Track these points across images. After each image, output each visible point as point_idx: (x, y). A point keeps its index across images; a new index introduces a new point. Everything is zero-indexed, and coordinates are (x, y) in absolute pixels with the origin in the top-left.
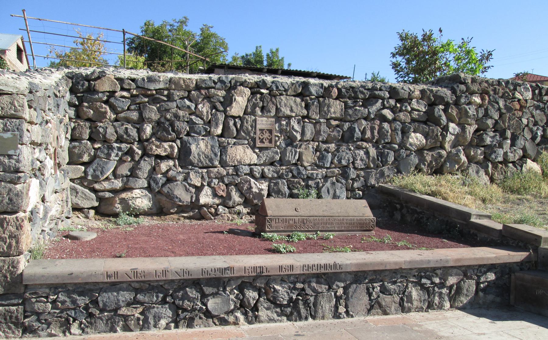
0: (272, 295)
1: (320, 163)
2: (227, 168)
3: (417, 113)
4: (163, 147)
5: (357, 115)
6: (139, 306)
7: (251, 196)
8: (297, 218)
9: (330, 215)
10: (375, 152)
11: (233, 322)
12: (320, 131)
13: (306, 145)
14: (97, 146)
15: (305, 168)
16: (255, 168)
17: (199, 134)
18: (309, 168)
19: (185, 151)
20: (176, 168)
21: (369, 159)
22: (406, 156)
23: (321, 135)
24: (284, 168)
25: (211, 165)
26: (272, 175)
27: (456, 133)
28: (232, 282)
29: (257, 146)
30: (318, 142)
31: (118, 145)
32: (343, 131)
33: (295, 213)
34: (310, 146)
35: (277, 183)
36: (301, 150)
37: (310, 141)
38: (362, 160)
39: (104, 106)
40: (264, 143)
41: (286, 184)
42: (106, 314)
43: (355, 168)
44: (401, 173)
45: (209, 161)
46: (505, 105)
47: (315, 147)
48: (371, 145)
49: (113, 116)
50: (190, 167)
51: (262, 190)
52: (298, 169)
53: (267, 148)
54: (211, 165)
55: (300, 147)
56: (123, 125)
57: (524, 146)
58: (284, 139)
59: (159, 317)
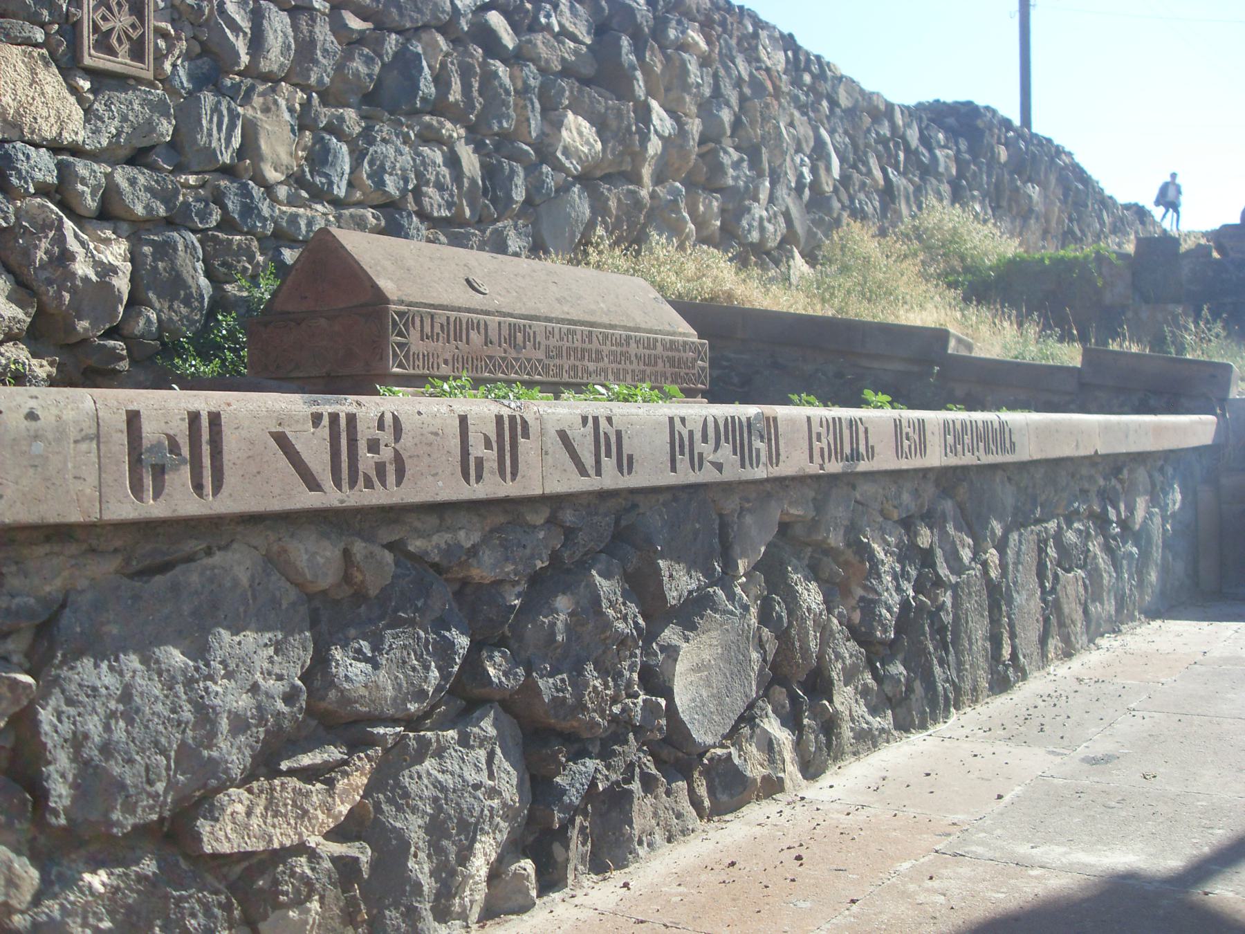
0: (860, 592)
1: (317, 179)
3: (572, 45)
5: (419, 11)
6: (334, 753)
7: (67, 296)
8: (493, 320)
9: (588, 318)
10: (475, 159)
11: (764, 778)
12: (313, 42)
13: (263, 94)
15: (269, 189)
16: (82, 167)
18: (282, 192)
21: (460, 187)
22: (557, 191)
23: (316, 62)
24: (192, 180)
27: (667, 134)
28: (749, 519)
29: (87, 61)
30: (305, 88)
32: (384, 64)
33: (475, 300)
34: (282, 103)
36: (250, 112)
37: (277, 81)
38: (440, 187)
40: (112, 52)
42: (98, 880)
43: (424, 216)
44: (547, 252)
46: (751, 75)
47: (297, 107)
48: (462, 132)
51: (113, 270)
52: (245, 193)
53: (121, 81)
55: (247, 100)
57: (787, 208)
58: (187, 56)
59: (463, 826)
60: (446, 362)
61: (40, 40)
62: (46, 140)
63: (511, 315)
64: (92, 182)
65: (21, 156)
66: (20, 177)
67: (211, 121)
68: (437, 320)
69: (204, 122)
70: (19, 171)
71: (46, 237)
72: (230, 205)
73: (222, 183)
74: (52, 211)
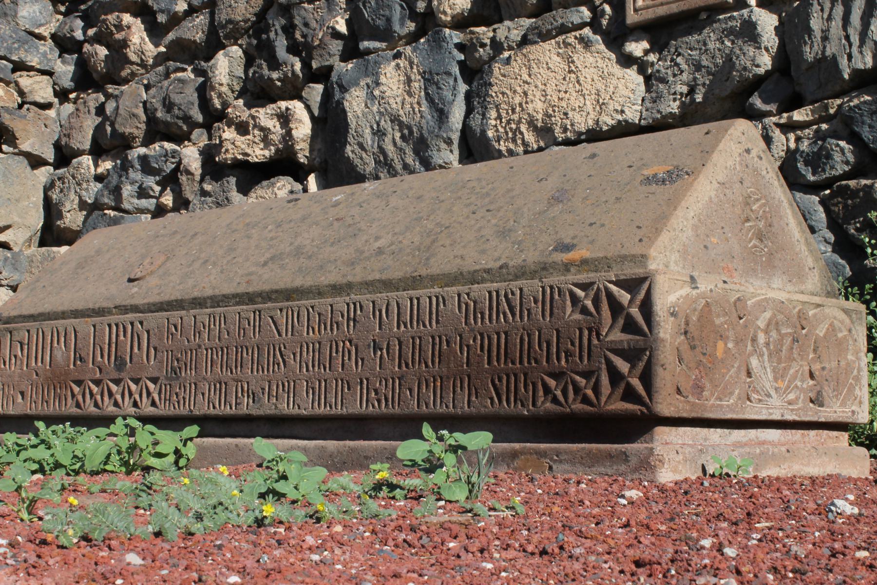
4: (255, 126)
14: (107, 165)
17: (385, 34)
19: (331, 122)
31: (142, 150)
39: (127, 18)
45: (416, 152)
49: (151, 50)
56: (167, 75)
60: (22, 394)
61: (577, 20)
62: (582, 133)
67: (830, 18)
68: (16, 337)
69: (816, 24)
72: (866, 134)
73: (856, 102)
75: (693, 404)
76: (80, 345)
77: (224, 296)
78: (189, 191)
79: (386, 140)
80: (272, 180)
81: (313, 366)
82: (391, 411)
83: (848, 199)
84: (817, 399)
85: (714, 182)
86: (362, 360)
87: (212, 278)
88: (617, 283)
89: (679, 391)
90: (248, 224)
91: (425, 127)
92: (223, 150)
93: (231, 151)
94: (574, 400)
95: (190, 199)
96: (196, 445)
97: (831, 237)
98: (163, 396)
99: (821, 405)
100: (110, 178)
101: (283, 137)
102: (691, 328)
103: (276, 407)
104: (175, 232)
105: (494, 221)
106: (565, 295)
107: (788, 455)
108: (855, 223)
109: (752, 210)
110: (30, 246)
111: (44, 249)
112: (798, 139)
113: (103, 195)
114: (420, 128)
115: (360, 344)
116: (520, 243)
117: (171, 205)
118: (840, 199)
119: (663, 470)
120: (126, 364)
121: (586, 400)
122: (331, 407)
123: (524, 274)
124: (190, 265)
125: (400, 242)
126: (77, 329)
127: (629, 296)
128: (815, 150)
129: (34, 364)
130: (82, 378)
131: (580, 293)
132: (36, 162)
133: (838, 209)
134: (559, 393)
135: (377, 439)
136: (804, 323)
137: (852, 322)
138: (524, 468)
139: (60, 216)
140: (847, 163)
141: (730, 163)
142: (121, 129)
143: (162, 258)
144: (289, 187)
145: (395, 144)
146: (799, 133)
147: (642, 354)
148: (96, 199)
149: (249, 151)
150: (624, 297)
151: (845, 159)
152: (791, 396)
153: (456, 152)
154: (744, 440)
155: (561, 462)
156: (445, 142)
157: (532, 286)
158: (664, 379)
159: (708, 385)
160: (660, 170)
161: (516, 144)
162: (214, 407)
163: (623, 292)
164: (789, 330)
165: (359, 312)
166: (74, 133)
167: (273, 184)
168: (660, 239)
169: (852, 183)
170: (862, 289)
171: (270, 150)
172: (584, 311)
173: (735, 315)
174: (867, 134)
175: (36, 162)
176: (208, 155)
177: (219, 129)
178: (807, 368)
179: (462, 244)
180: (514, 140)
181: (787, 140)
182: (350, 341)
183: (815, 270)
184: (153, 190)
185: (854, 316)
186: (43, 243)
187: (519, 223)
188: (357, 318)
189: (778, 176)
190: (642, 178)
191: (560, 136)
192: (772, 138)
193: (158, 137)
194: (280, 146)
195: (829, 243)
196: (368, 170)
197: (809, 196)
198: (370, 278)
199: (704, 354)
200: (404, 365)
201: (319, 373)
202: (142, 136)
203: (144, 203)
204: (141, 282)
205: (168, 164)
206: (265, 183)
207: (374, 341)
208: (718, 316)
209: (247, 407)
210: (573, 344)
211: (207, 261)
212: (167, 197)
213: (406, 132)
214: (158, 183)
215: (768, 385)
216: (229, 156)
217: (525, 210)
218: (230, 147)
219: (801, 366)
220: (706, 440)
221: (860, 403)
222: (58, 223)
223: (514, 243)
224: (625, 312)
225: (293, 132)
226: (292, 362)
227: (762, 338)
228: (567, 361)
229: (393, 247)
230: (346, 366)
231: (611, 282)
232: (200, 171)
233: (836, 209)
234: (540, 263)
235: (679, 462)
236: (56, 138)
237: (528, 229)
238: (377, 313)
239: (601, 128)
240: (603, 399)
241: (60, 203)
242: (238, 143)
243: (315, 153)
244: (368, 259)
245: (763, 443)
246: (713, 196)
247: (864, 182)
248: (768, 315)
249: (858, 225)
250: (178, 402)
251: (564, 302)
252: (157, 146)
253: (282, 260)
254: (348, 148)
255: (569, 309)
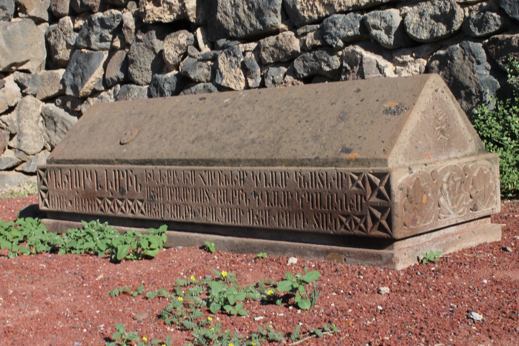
2: (301, 31)
4: (164, 2)
14: (80, 23)
20: (200, 50)
25: (259, 26)
26: (432, 31)
31: (100, 15)
35: (447, 54)
41: (483, 54)
45: (257, 17)
50: (222, 42)
54: (259, 26)
60: (71, 202)
63: (126, 162)
64: (384, 25)
65: (330, 24)
66: (332, 37)
68: (64, 172)
70: (331, 35)
71: (353, 72)
72: (508, 9)
74: (357, 53)
75: (413, 229)
76: (99, 179)
77: (174, 160)
78: (130, 39)
79: (239, 10)
80: (177, 33)
81: (224, 201)
82: (265, 226)
83: (497, 46)
84: (474, 208)
85: (420, 113)
86: (249, 200)
87: (166, 147)
88: (373, 174)
89: (405, 225)
90: (180, 113)
91: (261, 3)
92: (147, 16)
93: (152, 16)
94: (355, 228)
95: (131, 43)
96: (166, 235)
97: (489, 66)
98: (147, 209)
99: (476, 210)
100: (82, 31)
101: (181, 8)
102: (410, 193)
103: (207, 220)
104: (140, 113)
105: (310, 129)
106: (348, 178)
107: (460, 240)
108: (502, 59)
109: (439, 121)
110: (41, 70)
111: (49, 72)
112: (470, 11)
113: (80, 41)
114: (259, 4)
115: (247, 192)
116: (324, 145)
117: (119, 46)
118: (493, 46)
119: (399, 264)
120: (125, 191)
121: (360, 229)
122: (235, 222)
123: (327, 163)
124: (153, 138)
125: (263, 137)
126: (97, 171)
127: (379, 181)
128: (480, 18)
129: (75, 187)
130: (102, 197)
131: (356, 177)
132: (38, 21)
133: (492, 51)
134: (347, 224)
135: (259, 238)
136: (466, 172)
137: (492, 163)
138: (333, 259)
139: (56, 53)
140: (497, 25)
141: (427, 100)
142: (86, 2)
143: (137, 131)
144: (186, 37)
145: (245, 12)
146: (471, 7)
147: (386, 208)
148: (76, 43)
149: (162, 16)
150: (377, 181)
151: (496, 23)
152: (461, 210)
153: (280, 17)
154: (438, 236)
155: (350, 257)
156: (273, 11)
157: (331, 169)
158: (397, 221)
159: (419, 218)
160: (392, 104)
161: (313, 13)
162: (174, 217)
163: (376, 178)
164: (459, 178)
165: (245, 176)
166: (59, 4)
167: (177, 35)
168: (393, 150)
169: (500, 36)
170: (505, 102)
171: (174, 15)
172: (358, 186)
173: (432, 179)
174: (508, 9)
175: (38, 21)
176: (139, 17)
177: (143, 3)
178: (468, 195)
179: (295, 142)
180: (312, 11)
181: (464, 11)
182: (242, 191)
183: (473, 141)
184: (107, 37)
185: (493, 160)
186: (48, 68)
187: (323, 132)
188: (245, 179)
189: (452, 98)
190: (384, 109)
191: (338, 9)
192: (455, 11)
193: (108, 7)
194: (180, 13)
195: (488, 70)
196: (230, 27)
197: (476, 44)
198: (249, 157)
199: (417, 204)
200: (270, 205)
201: (227, 204)
202: (98, 6)
203: (104, 45)
204: (127, 145)
205: (115, 22)
206: (173, 34)
207: (254, 192)
208: (423, 182)
209: (191, 218)
210: (353, 201)
211: (161, 136)
212: (117, 42)
213: (250, 5)
214: (110, 33)
215: (449, 209)
216: (151, 19)
217: (326, 123)
218: (151, 14)
219: (466, 194)
220: (419, 242)
221: (496, 203)
222: (56, 56)
223: (321, 144)
224: (378, 189)
225: (186, 5)
226: (213, 198)
227: (445, 186)
228: (351, 209)
229: (260, 139)
230: (241, 202)
231: (370, 173)
232: (134, 27)
233: (492, 51)
234: (335, 158)
235: (406, 259)
236: (48, 6)
237: (328, 136)
238: (255, 178)
239: (361, 5)
240: (369, 229)
241: (55, 45)
242: (155, 12)
243: (200, 16)
244: (247, 145)
245: (446, 236)
246: (419, 120)
247: (507, 36)
248: (448, 174)
249: (504, 60)
250: (155, 213)
251: (348, 181)
252: (108, 12)
253: (202, 140)
254: (218, 15)
255: (350, 185)
